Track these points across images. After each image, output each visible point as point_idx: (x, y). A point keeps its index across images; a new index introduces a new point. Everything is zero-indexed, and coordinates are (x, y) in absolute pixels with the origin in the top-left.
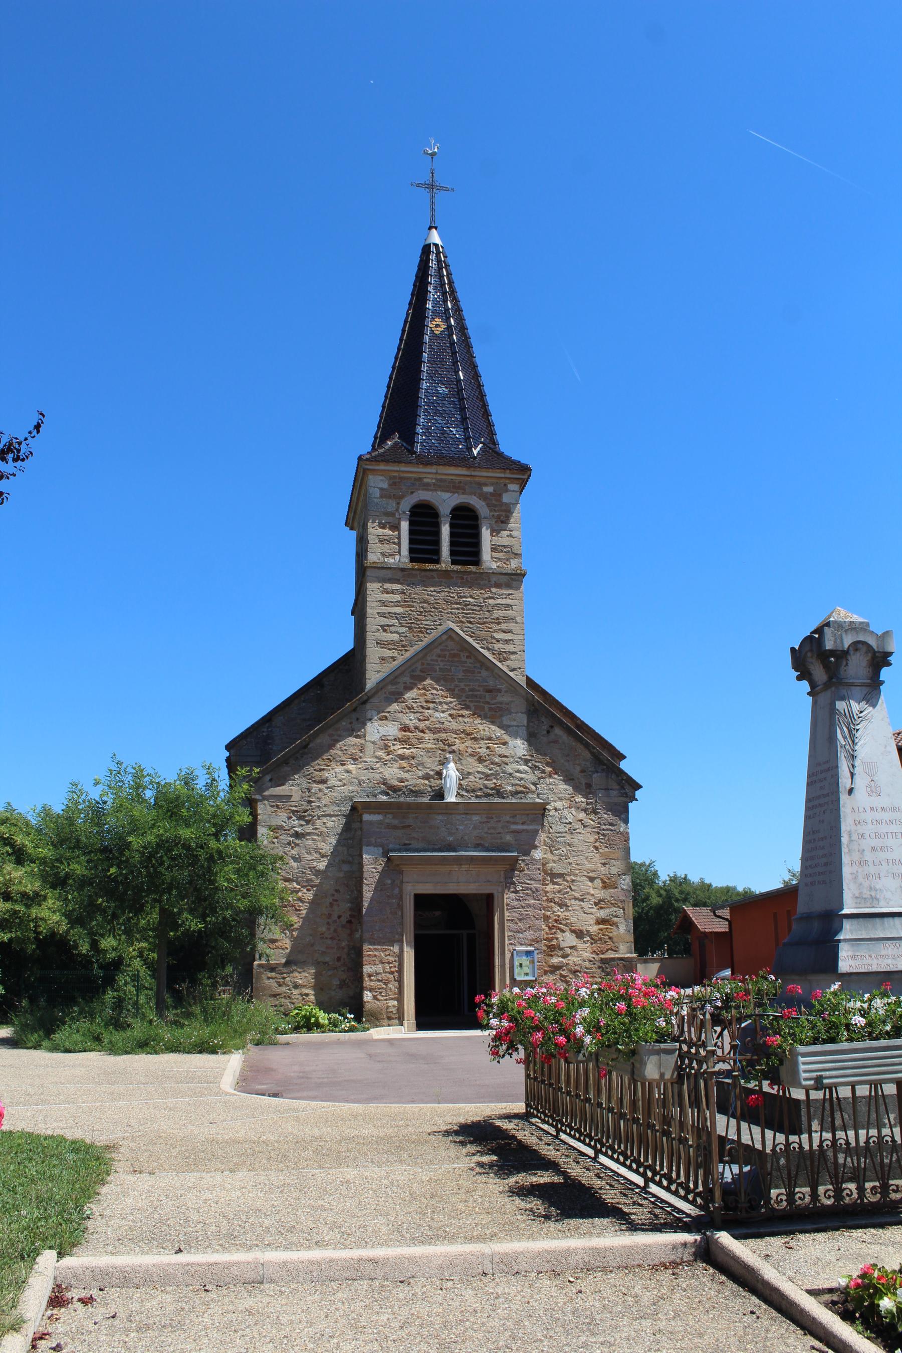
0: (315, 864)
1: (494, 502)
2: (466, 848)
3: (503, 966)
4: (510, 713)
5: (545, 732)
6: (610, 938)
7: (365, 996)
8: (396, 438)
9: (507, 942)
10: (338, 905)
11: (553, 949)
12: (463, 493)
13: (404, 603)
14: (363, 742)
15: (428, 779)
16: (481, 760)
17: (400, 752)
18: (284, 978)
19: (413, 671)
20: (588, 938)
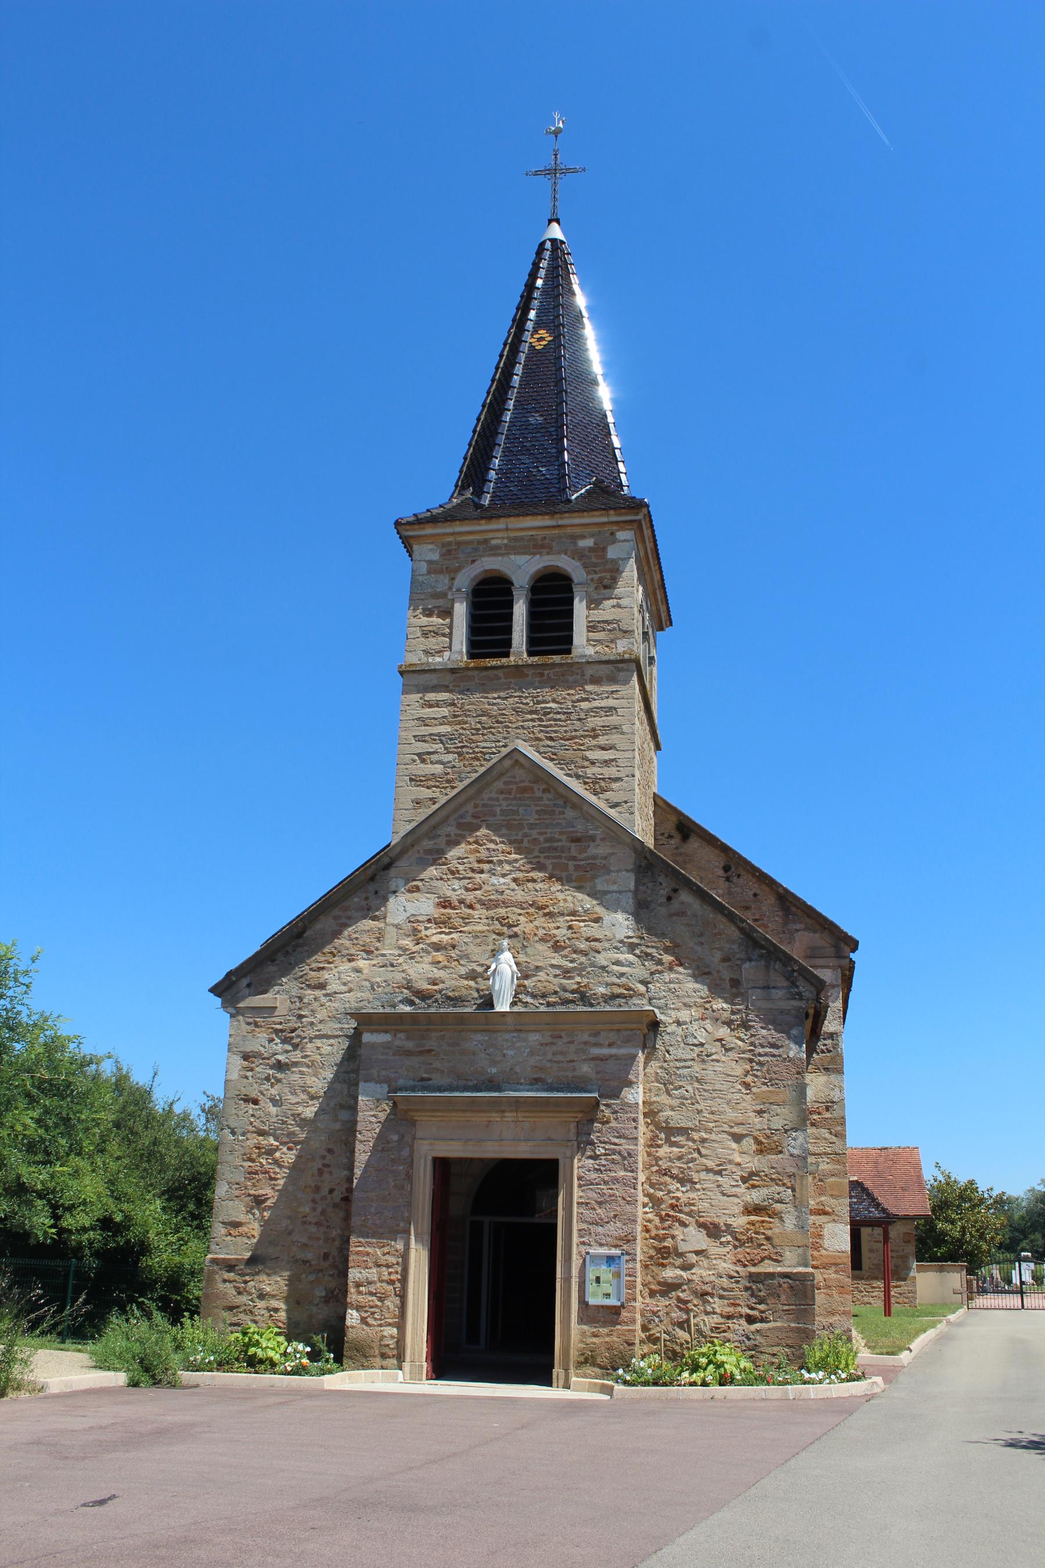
0: (300, 1109)
1: (594, 560)
2: (516, 1085)
3: (567, 1279)
4: (609, 872)
5: (664, 900)
6: (768, 1238)
7: (348, 1317)
8: (468, 494)
9: (575, 1239)
10: (331, 1173)
11: (663, 1254)
12: (548, 553)
14: (382, 925)
15: (474, 979)
16: (557, 947)
17: (435, 939)
18: (246, 1282)
19: (461, 817)
20: (729, 1238)
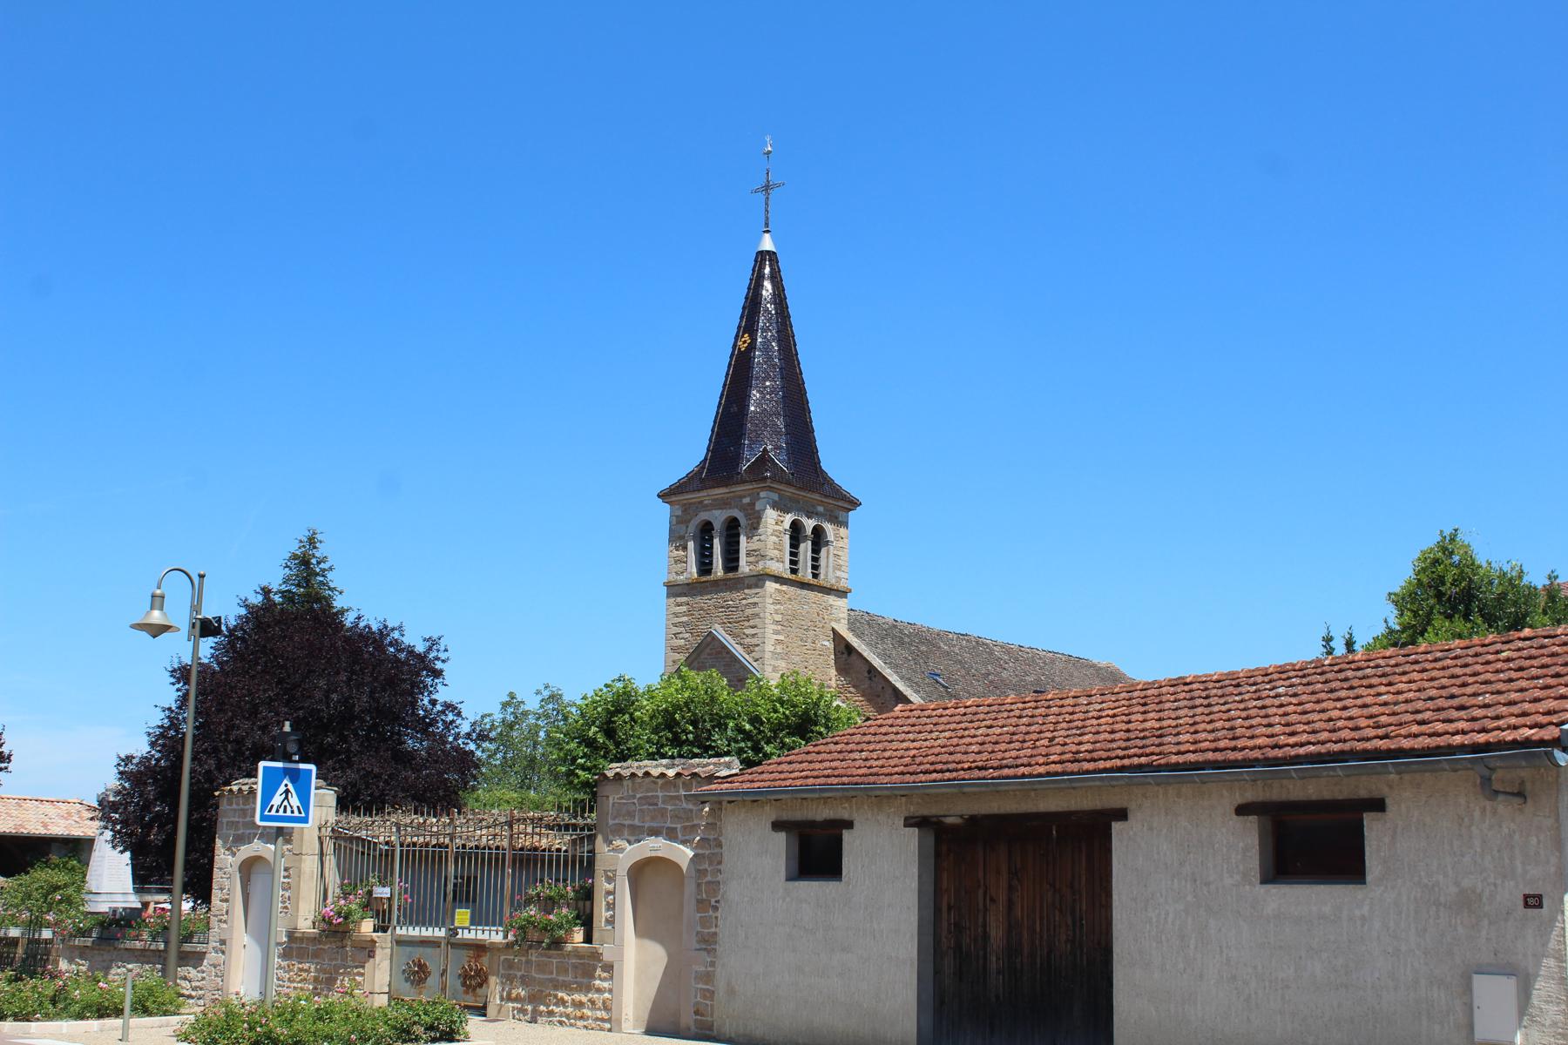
13: (689, 613)
